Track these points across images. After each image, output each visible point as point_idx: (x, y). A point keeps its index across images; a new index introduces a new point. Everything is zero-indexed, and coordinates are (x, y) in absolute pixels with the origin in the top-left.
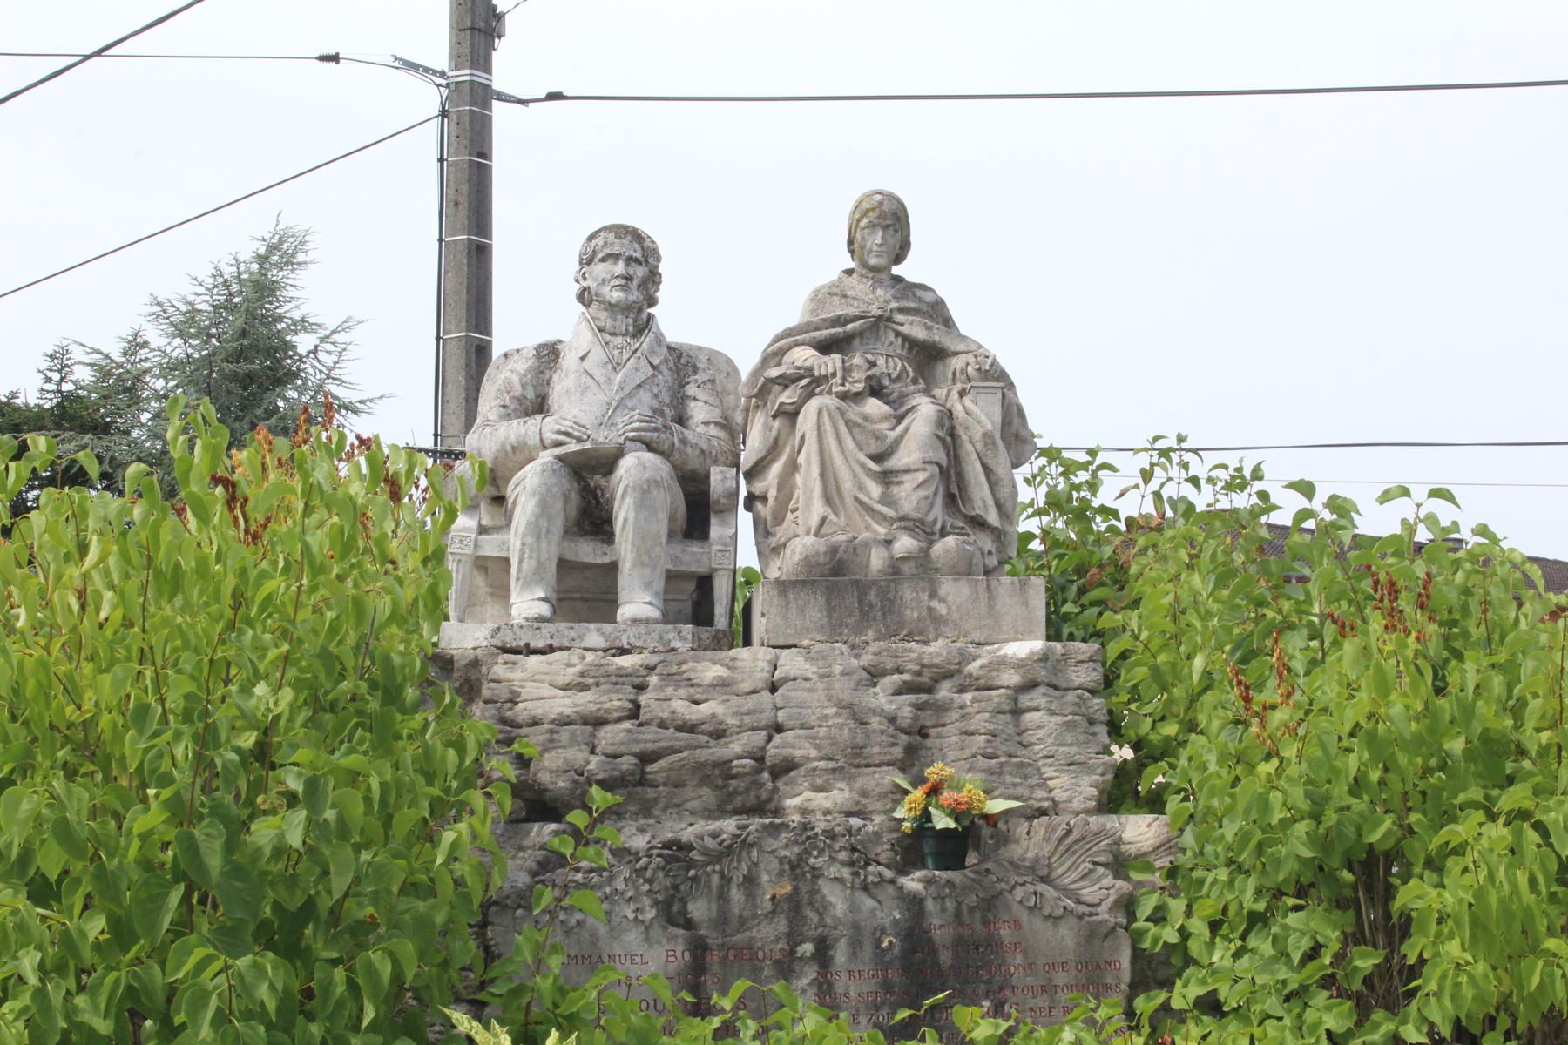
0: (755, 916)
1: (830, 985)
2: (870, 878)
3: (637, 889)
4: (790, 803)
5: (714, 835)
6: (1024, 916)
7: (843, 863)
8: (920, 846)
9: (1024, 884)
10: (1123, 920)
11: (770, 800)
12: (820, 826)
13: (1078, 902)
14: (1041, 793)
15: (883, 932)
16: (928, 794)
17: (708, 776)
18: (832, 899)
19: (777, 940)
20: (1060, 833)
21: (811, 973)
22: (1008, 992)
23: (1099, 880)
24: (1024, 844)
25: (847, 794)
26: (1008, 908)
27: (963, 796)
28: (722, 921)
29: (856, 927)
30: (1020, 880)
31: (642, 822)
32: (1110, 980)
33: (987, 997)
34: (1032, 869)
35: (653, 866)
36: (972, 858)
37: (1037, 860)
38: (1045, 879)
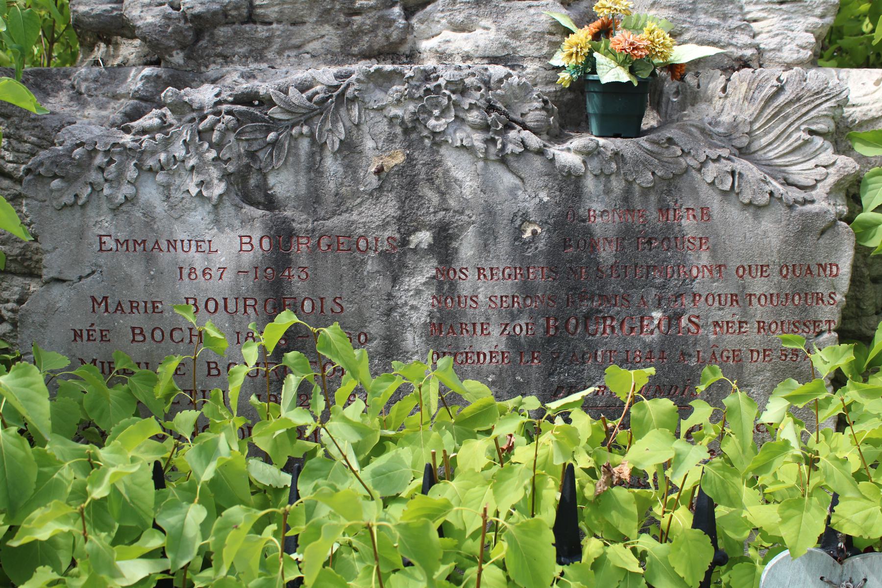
0: (355, 194)
1: (453, 285)
2: (510, 147)
3: (201, 156)
4: (425, 45)
5: (303, 88)
6: (715, 203)
7: (475, 127)
8: (577, 104)
9: (718, 159)
10: (844, 209)
11: (402, 41)
12: (446, 75)
13: (787, 183)
14: (743, 38)
15: (525, 218)
16: (596, 37)
17: (327, 11)
18: (459, 174)
19: (384, 225)
20: (768, 91)
21: (428, 269)
22: (687, 301)
23: (815, 154)
24: (718, 103)
25: (492, 34)
26: (694, 191)
27: (642, 39)
28: (313, 200)
29: (489, 211)
30: (714, 153)
31: (253, 66)
32: (822, 288)
33: (659, 306)
34: (728, 137)
35: (220, 126)
36: (650, 120)
37: (734, 125)
38: (744, 152)
